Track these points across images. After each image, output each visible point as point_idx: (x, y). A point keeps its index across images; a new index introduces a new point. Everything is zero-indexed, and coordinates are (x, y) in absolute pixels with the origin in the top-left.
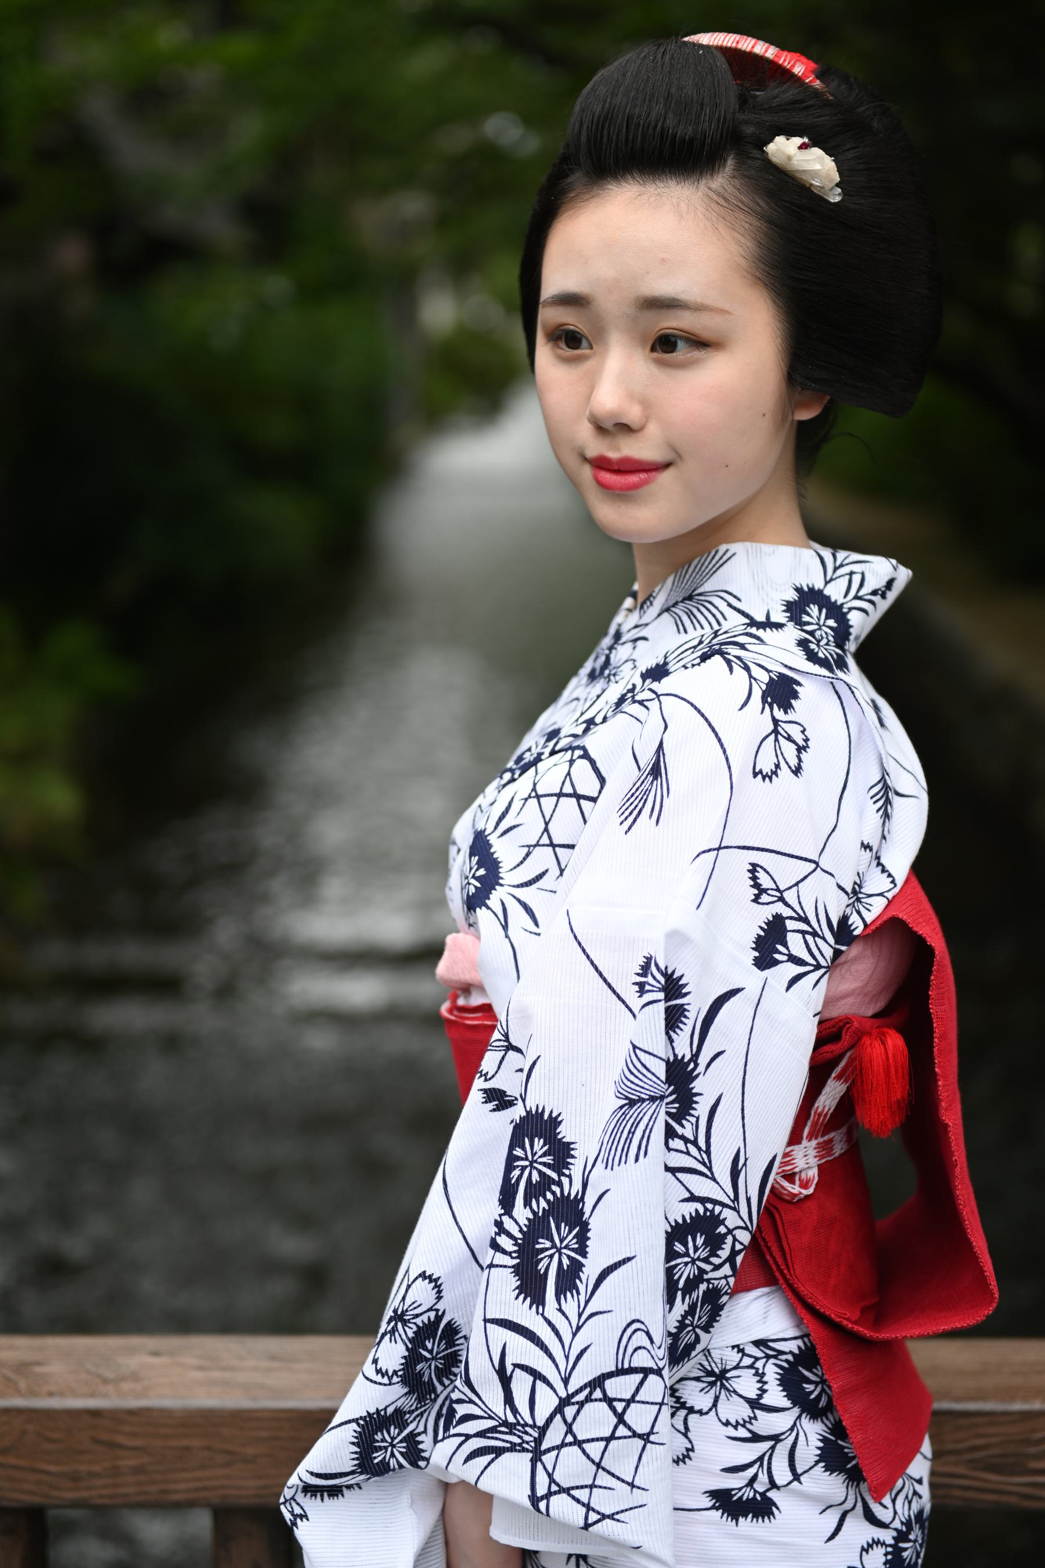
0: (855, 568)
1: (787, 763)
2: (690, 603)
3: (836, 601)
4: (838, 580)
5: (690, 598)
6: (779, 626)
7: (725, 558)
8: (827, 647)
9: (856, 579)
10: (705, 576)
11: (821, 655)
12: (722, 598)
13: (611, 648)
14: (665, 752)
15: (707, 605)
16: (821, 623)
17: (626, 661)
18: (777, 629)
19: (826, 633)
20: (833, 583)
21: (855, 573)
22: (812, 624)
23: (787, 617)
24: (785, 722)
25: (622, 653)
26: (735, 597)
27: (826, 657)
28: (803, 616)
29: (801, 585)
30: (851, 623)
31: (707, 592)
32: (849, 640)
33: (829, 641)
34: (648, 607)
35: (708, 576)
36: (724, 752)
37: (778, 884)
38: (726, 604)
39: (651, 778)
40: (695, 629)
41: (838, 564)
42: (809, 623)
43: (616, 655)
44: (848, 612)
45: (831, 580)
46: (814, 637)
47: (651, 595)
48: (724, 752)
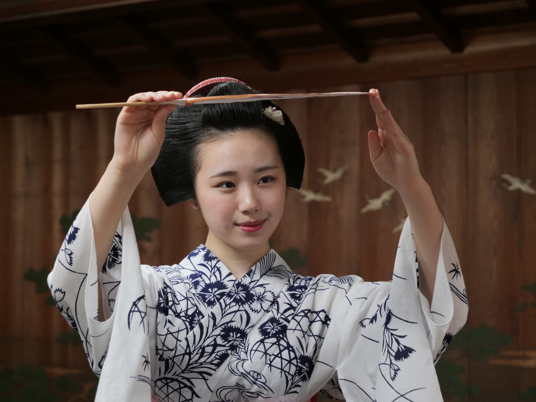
5: (270, 269)
34: (253, 275)
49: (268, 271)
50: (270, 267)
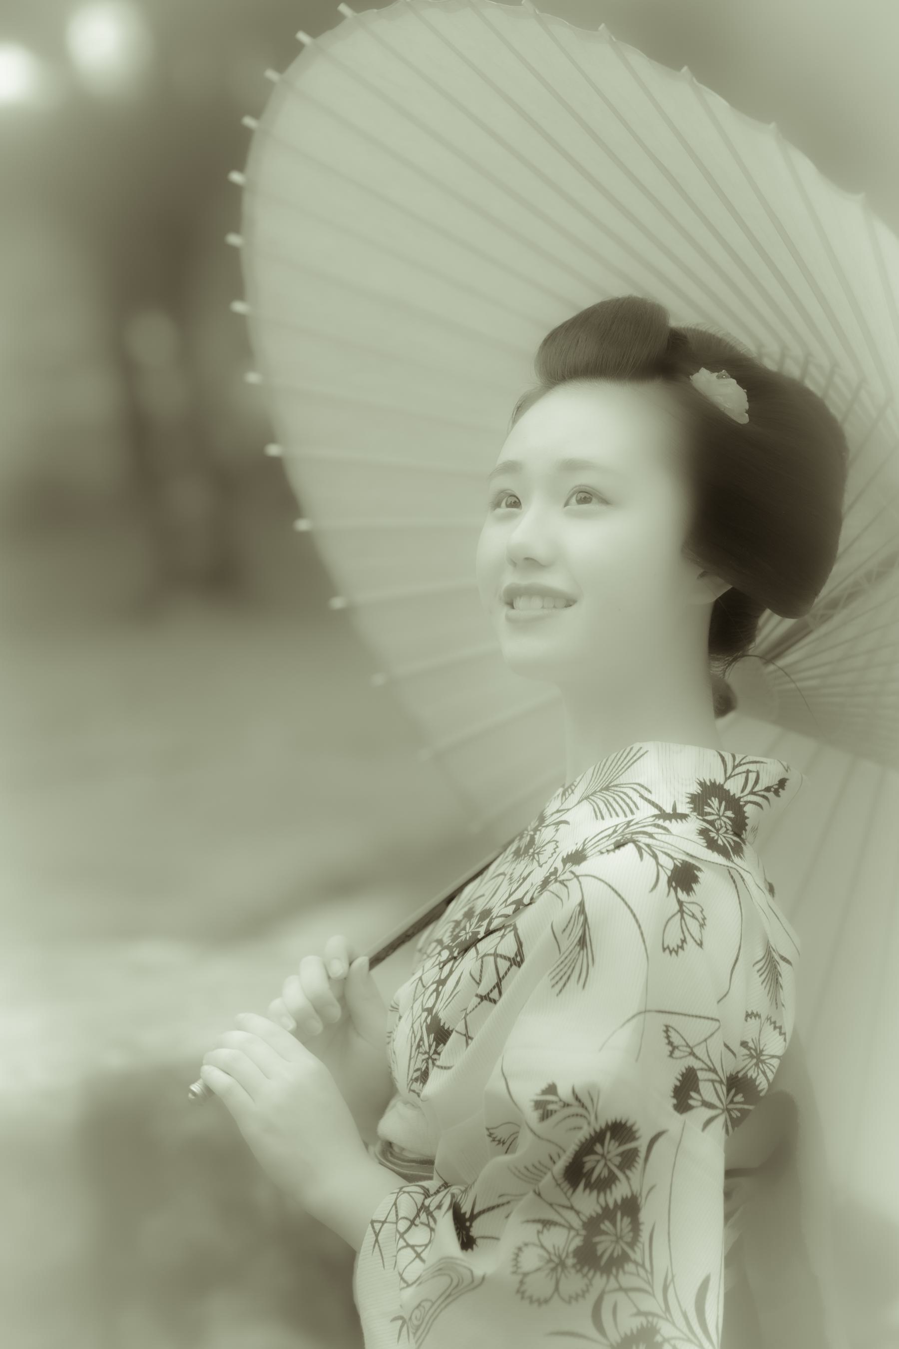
0: (752, 767)
1: (693, 938)
2: (607, 793)
3: (734, 795)
4: (736, 777)
5: (607, 788)
6: (683, 817)
7: (638, 755)
8: (725, 835)
9: (752, 777)
10: (621, 770)
11: (720, 842)
12: (635, 790)
13: (536, 830)
14: (590, 926)
15: (622, 795)
16: (721, 814)
17: (549, 842)
18: (682, 821)
19: (725, 822)
20: (732, 779)
21: (751, 771)
22: (713, 814)
23: (691, 808)
24: (690, 903)
25: (546, 834)
26: (646, 789)
27: (724, 844)
28: (705, 807)
29: (704, 780)
30: (746, 815)
31: (622, 784)
32: (746, 830)
33: (727, 830)
34: (569, 795)
35: (623, 770)
36: (640, 927)
37: (688, 1042)
38: (638, 795)
39: (578, 949)
40: (611, 816)
41: (737, 762)
42: (710, 814)
43: (540, 836)
44: (745, 805)
45: (730, 777)
46: (714, 826)
47: (573, 784)
48: (640, 927)
49: (602, 789)
50: (611, 782)
